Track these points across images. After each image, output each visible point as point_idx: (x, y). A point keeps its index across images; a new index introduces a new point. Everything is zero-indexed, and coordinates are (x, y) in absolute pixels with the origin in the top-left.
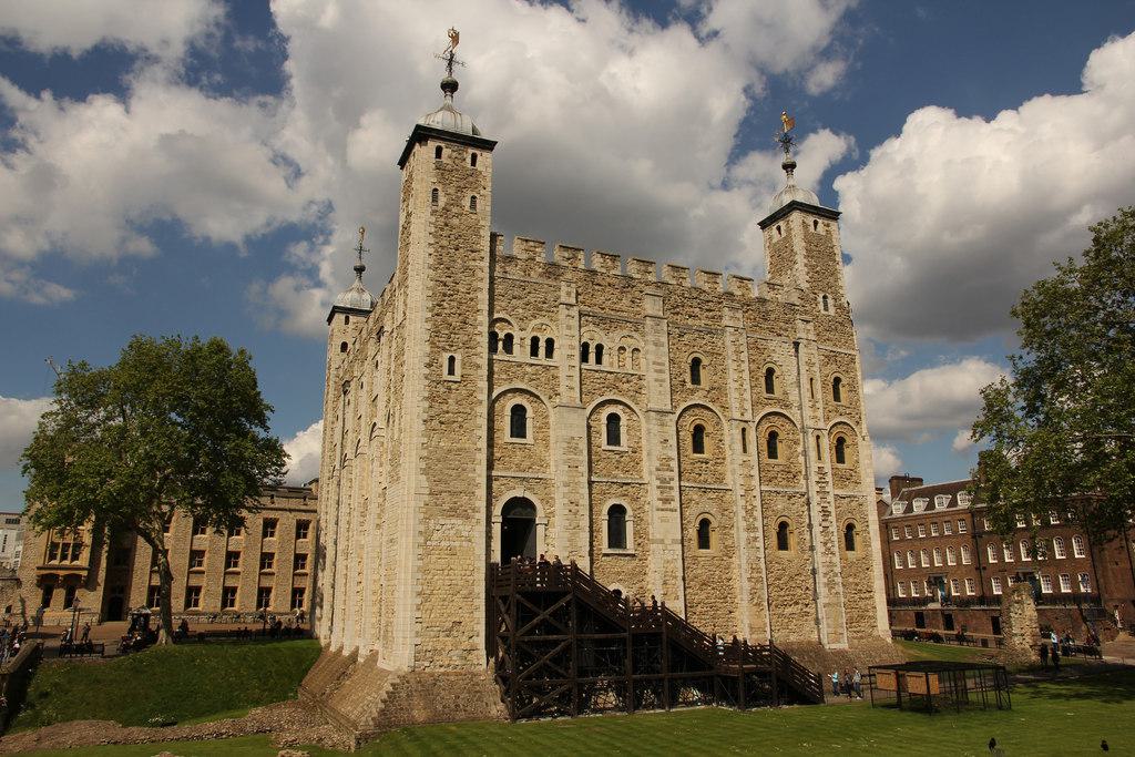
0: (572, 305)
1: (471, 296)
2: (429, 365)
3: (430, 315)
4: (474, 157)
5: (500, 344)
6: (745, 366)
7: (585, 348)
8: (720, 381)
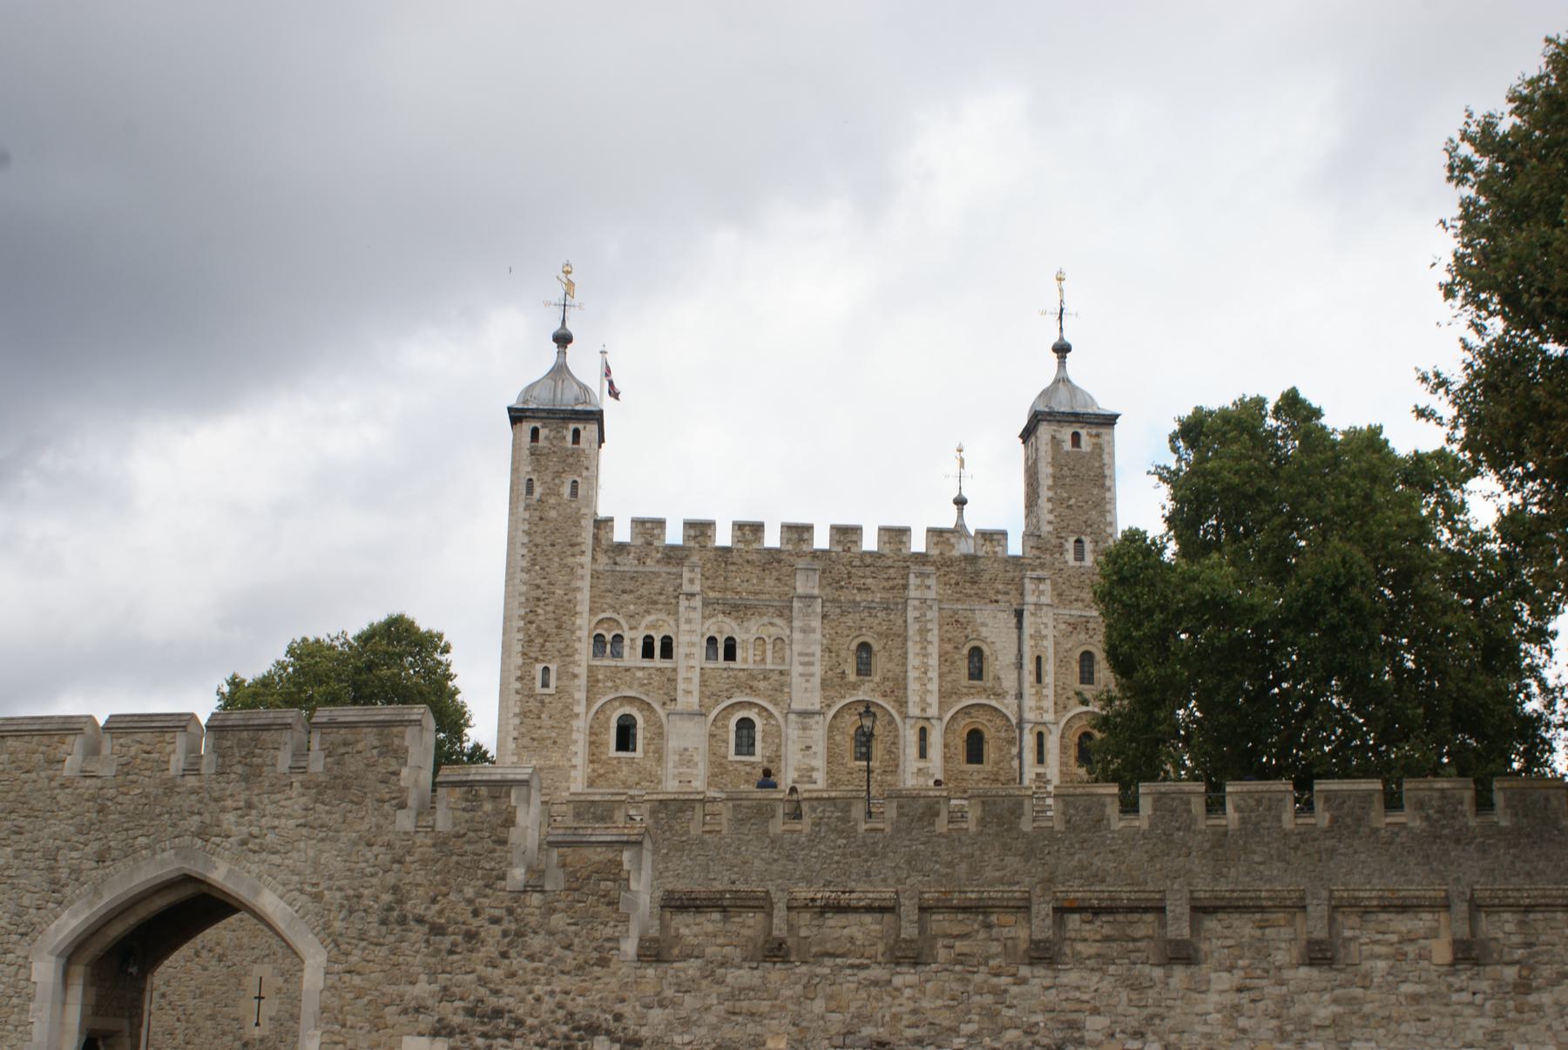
0: (693, 595)
3: (521, 624)
4: (576, 433)
6: (934, 650)
7: (712, 641)
8: (898, 670)
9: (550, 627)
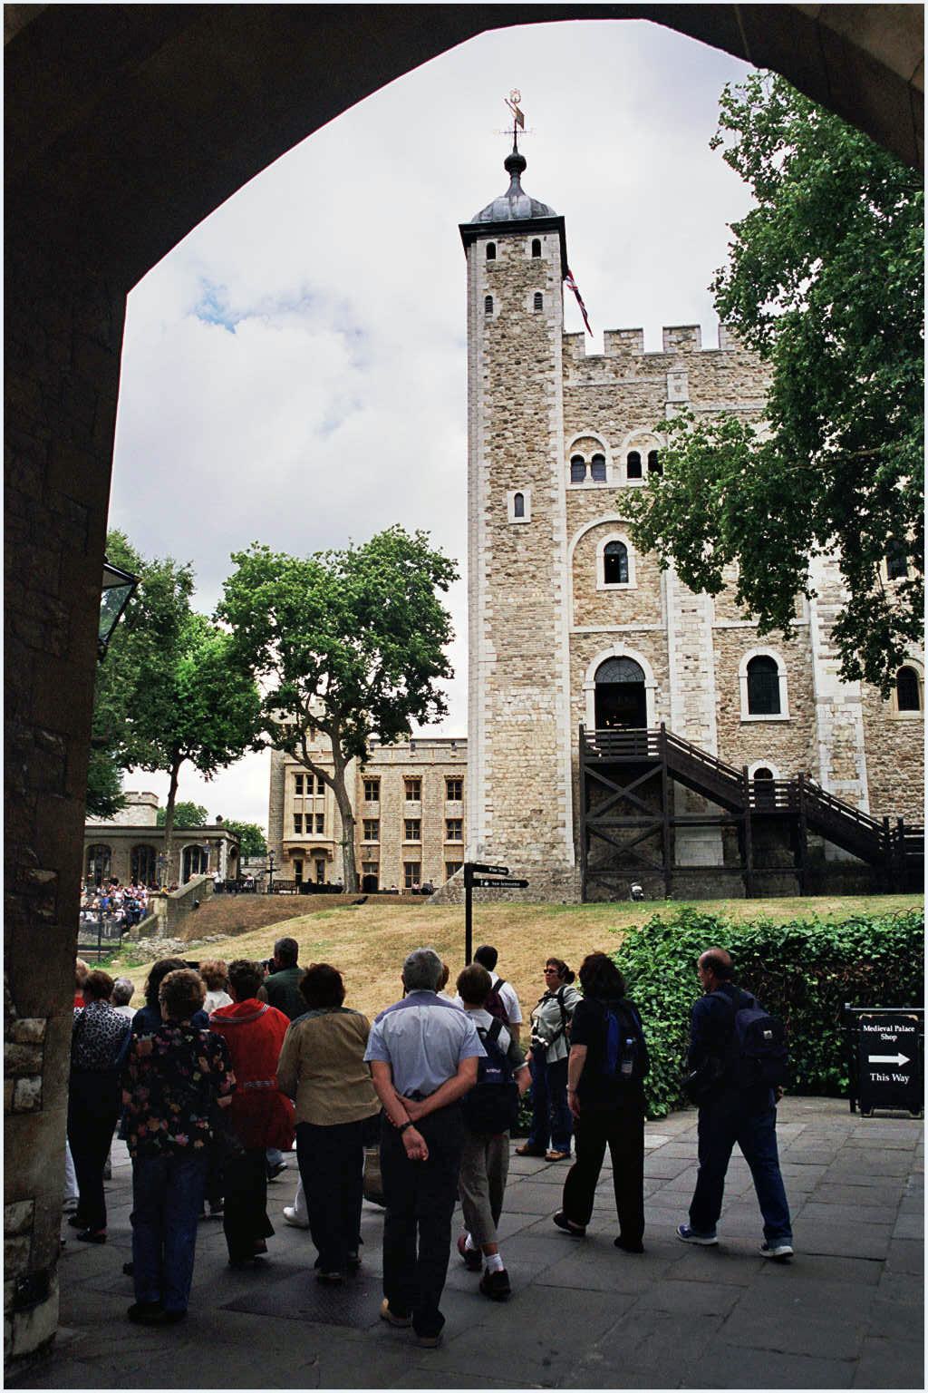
1: (540, 416)
2: (489, 509)
3: (488, 449)
5: (588, 468)
9: (521, 451)
